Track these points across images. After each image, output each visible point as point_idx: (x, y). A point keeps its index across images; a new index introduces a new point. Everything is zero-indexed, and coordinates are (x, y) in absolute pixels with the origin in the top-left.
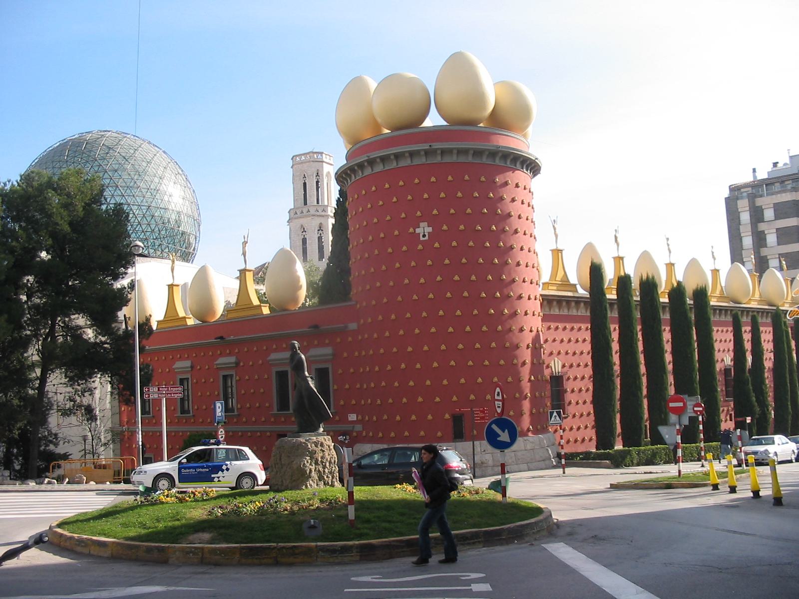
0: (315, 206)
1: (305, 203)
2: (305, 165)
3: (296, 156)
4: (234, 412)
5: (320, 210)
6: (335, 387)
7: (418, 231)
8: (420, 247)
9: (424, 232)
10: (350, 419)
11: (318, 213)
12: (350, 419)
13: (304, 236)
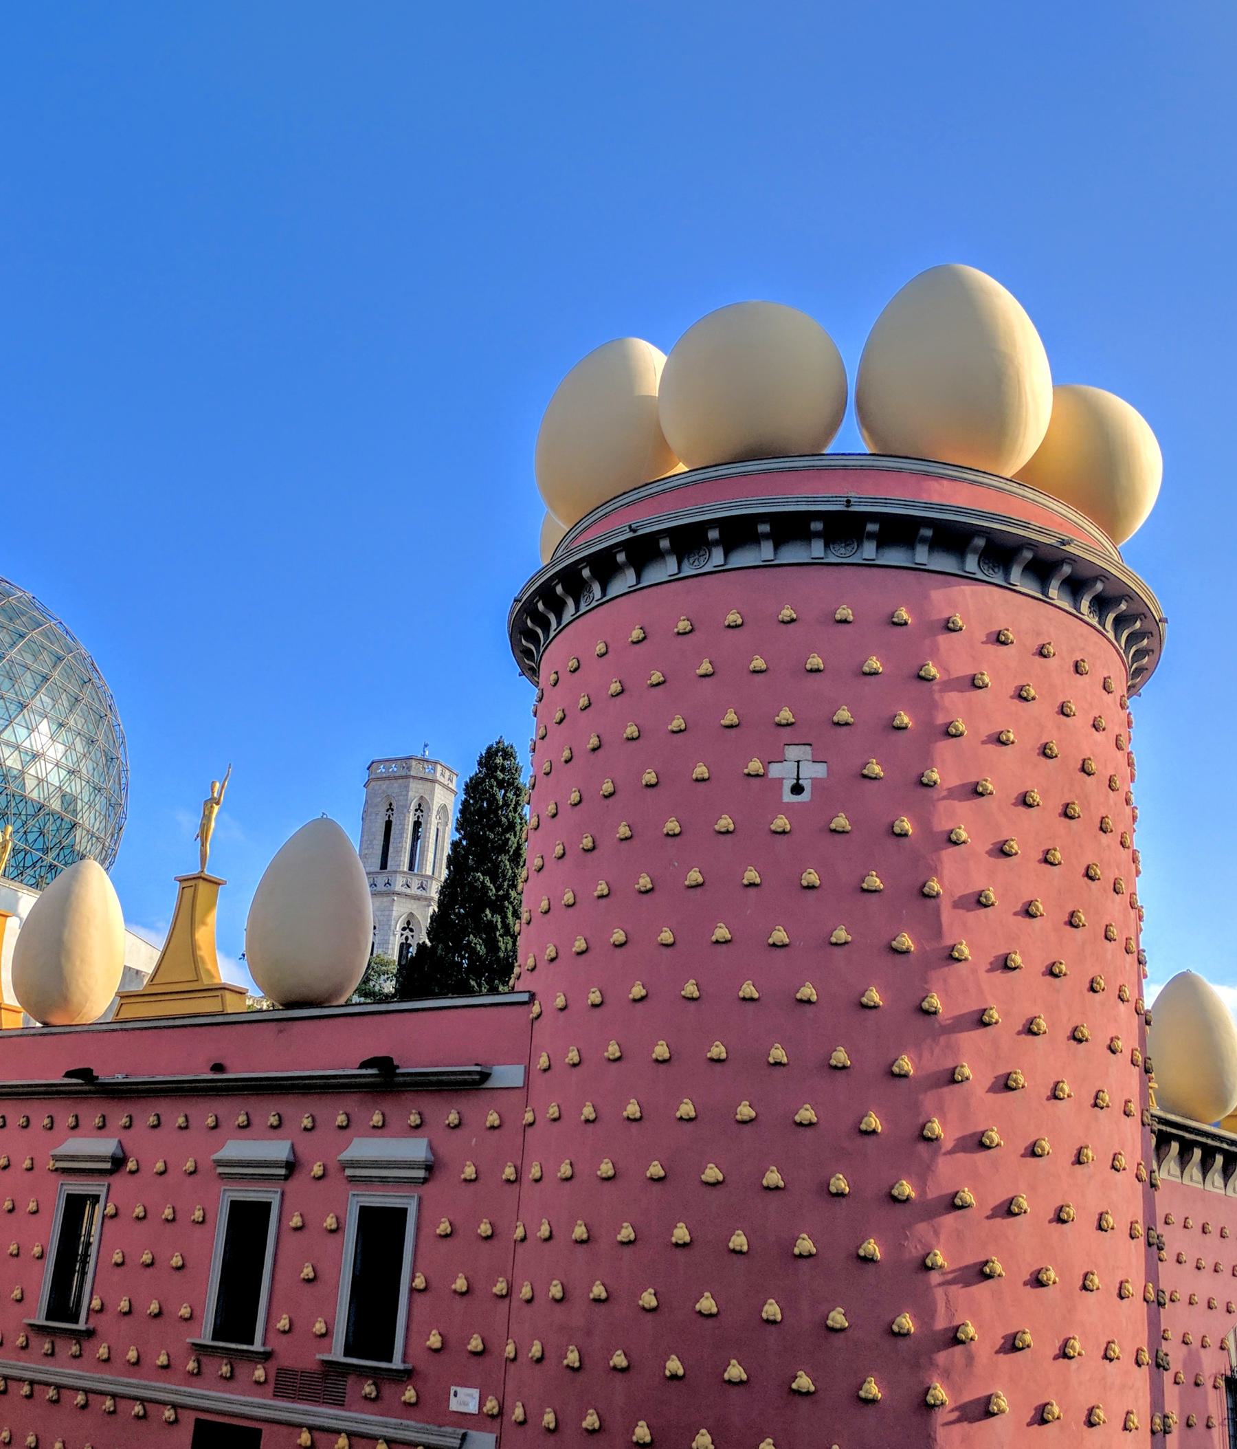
0: (404, 873)
1: (384, 865)
2: (396, 784)
3: (379, 761)
4: (77, 1322)
5: (415, 883)
6: (420, 1282)
7: (775, 771)
8: (781, 822)
9: (798, 779)
10: (454, 1405)
11: (408, 891)
12: (454, 1405)
13: (389, 817)
